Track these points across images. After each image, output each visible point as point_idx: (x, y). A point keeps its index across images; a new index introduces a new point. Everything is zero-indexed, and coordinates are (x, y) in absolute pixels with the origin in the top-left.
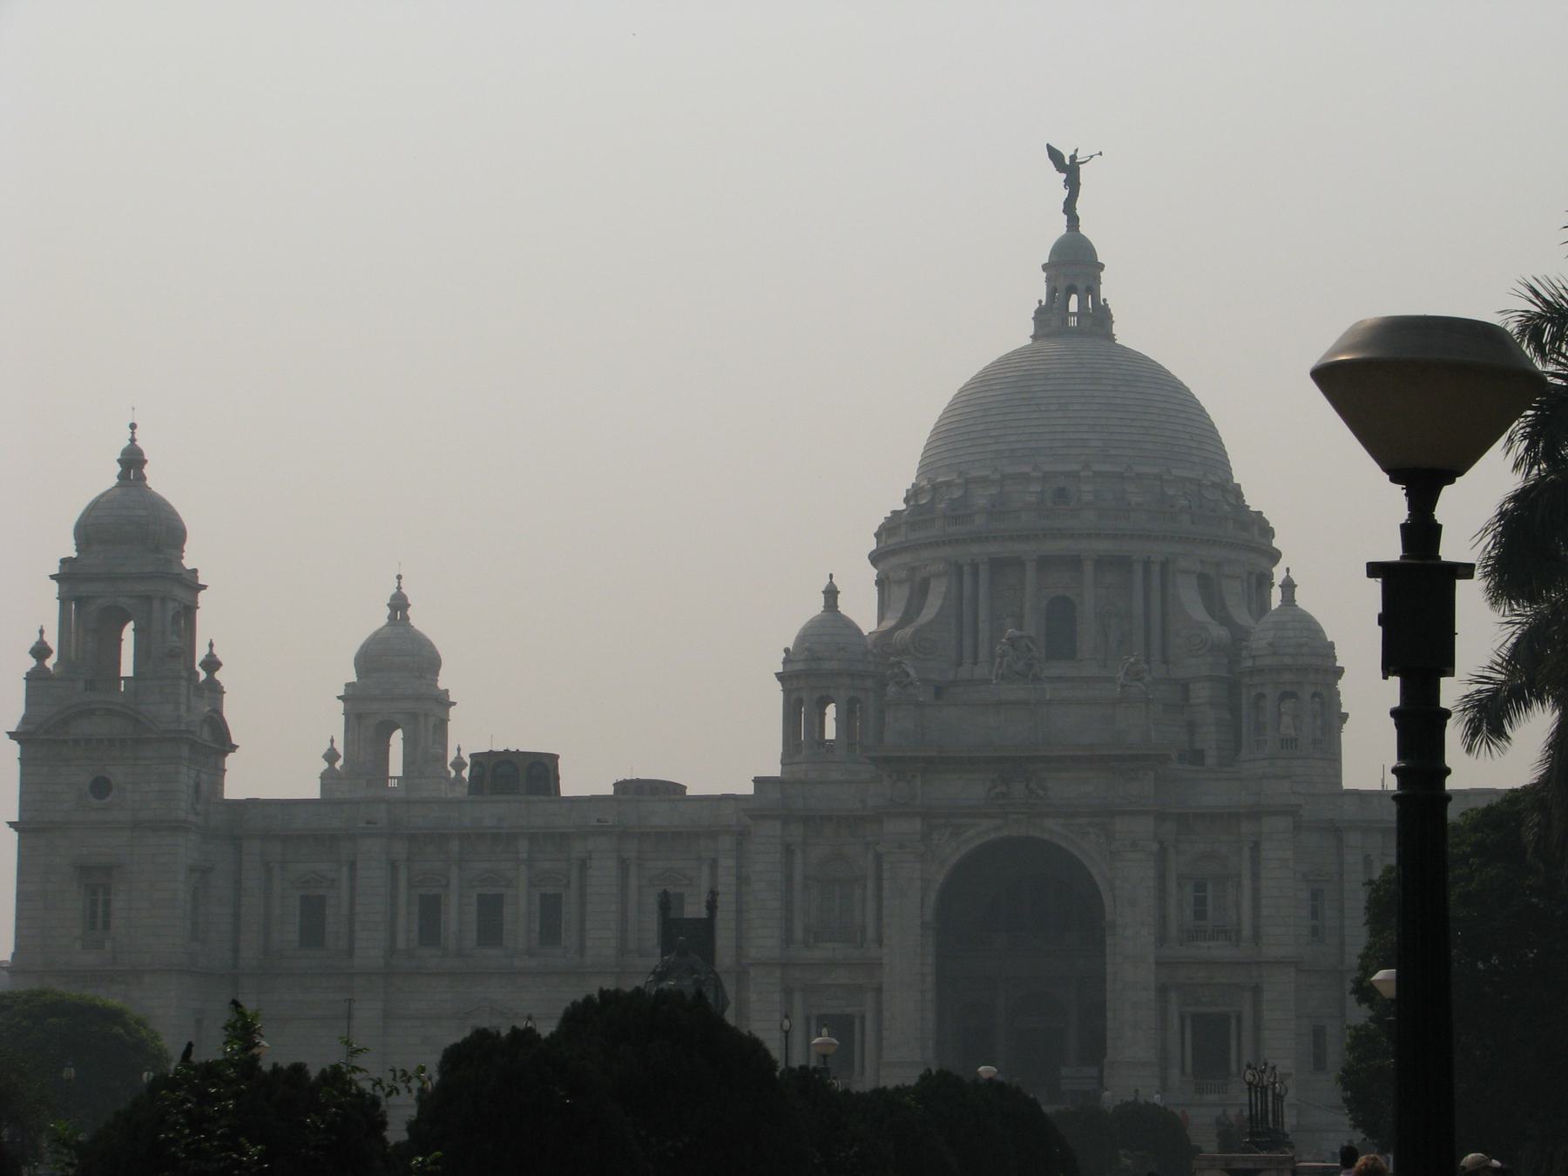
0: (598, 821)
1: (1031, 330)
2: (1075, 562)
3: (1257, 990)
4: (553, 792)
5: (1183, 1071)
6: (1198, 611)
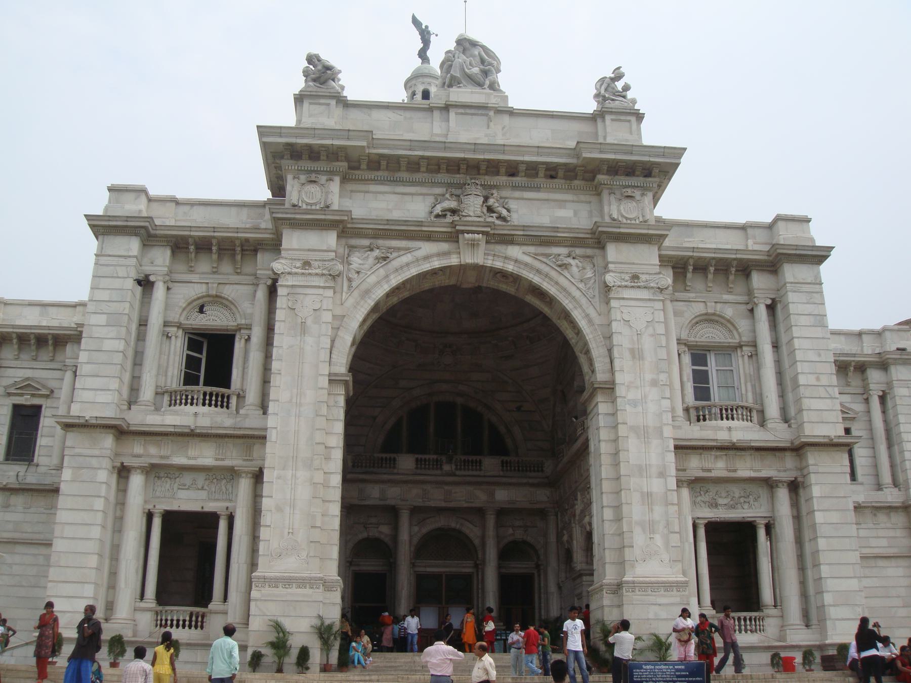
3: (795, 487)
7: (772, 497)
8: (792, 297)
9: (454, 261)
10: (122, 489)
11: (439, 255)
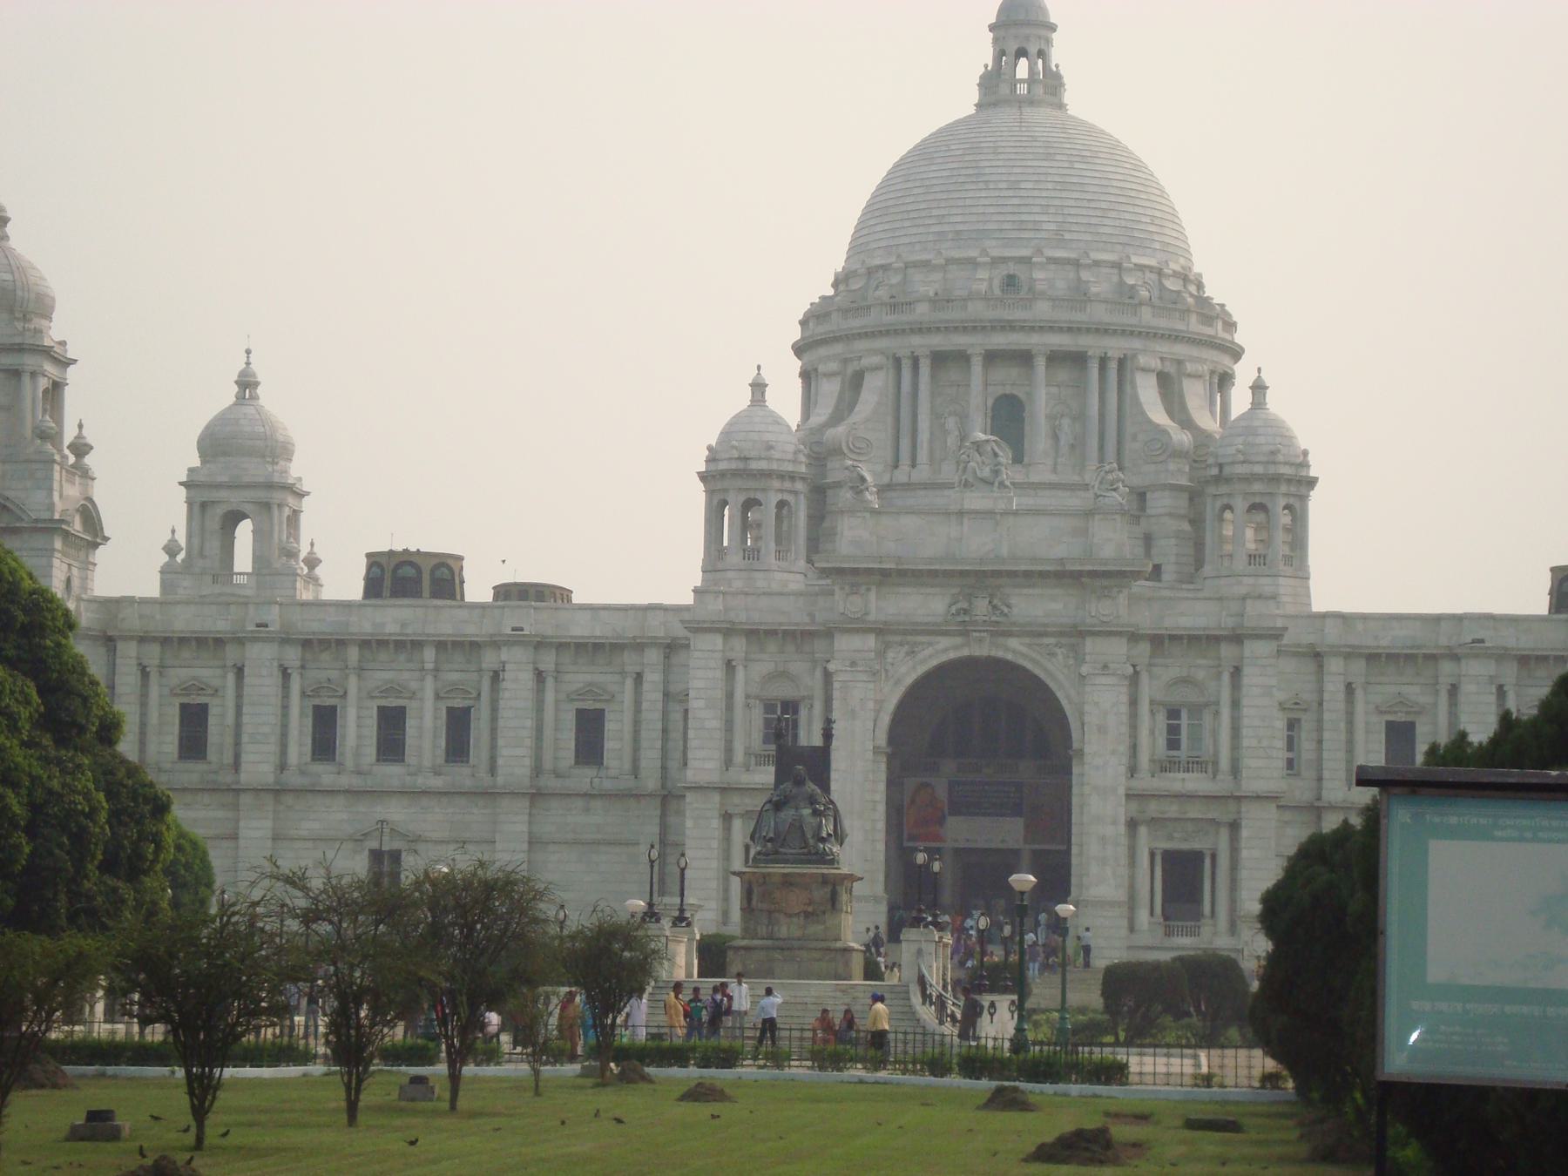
0: (513, 630)
1: (974, 96)
2: (1024, 358)
3: (1234, 827)
4: (458, 597)
5: (1152, 913)
6: (1159, 416)
7: (1217, 833)
8: (1247, 670)
9: (965, 652)
10: (727, 829)
11: (956, 648)
